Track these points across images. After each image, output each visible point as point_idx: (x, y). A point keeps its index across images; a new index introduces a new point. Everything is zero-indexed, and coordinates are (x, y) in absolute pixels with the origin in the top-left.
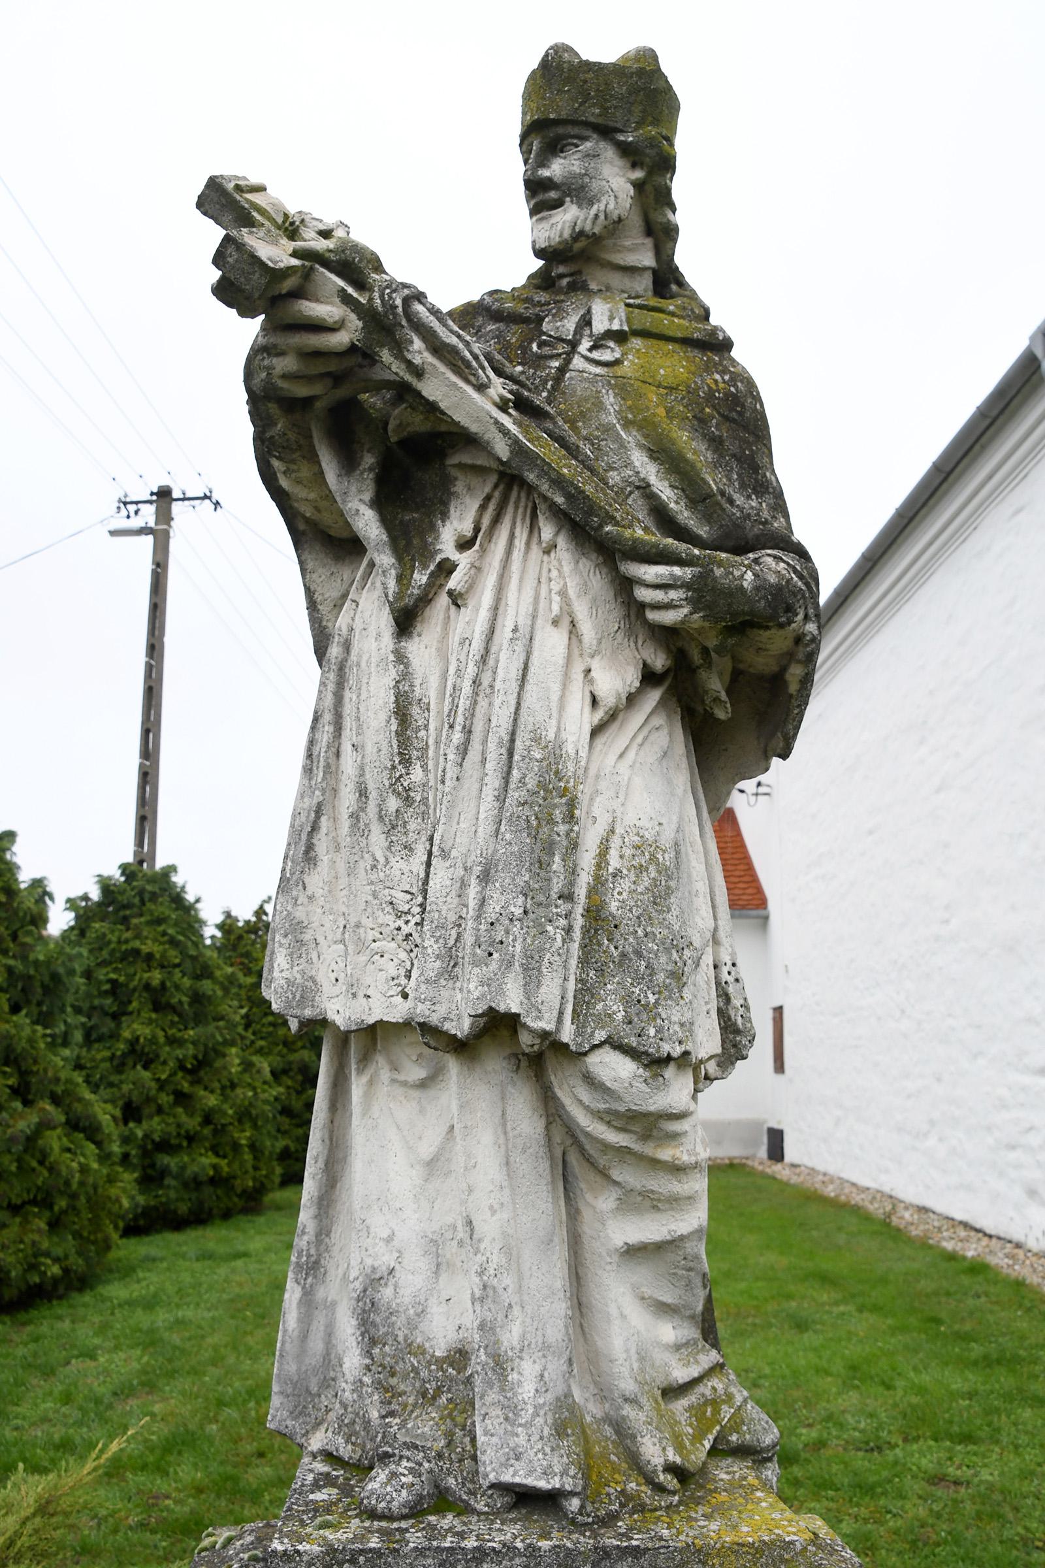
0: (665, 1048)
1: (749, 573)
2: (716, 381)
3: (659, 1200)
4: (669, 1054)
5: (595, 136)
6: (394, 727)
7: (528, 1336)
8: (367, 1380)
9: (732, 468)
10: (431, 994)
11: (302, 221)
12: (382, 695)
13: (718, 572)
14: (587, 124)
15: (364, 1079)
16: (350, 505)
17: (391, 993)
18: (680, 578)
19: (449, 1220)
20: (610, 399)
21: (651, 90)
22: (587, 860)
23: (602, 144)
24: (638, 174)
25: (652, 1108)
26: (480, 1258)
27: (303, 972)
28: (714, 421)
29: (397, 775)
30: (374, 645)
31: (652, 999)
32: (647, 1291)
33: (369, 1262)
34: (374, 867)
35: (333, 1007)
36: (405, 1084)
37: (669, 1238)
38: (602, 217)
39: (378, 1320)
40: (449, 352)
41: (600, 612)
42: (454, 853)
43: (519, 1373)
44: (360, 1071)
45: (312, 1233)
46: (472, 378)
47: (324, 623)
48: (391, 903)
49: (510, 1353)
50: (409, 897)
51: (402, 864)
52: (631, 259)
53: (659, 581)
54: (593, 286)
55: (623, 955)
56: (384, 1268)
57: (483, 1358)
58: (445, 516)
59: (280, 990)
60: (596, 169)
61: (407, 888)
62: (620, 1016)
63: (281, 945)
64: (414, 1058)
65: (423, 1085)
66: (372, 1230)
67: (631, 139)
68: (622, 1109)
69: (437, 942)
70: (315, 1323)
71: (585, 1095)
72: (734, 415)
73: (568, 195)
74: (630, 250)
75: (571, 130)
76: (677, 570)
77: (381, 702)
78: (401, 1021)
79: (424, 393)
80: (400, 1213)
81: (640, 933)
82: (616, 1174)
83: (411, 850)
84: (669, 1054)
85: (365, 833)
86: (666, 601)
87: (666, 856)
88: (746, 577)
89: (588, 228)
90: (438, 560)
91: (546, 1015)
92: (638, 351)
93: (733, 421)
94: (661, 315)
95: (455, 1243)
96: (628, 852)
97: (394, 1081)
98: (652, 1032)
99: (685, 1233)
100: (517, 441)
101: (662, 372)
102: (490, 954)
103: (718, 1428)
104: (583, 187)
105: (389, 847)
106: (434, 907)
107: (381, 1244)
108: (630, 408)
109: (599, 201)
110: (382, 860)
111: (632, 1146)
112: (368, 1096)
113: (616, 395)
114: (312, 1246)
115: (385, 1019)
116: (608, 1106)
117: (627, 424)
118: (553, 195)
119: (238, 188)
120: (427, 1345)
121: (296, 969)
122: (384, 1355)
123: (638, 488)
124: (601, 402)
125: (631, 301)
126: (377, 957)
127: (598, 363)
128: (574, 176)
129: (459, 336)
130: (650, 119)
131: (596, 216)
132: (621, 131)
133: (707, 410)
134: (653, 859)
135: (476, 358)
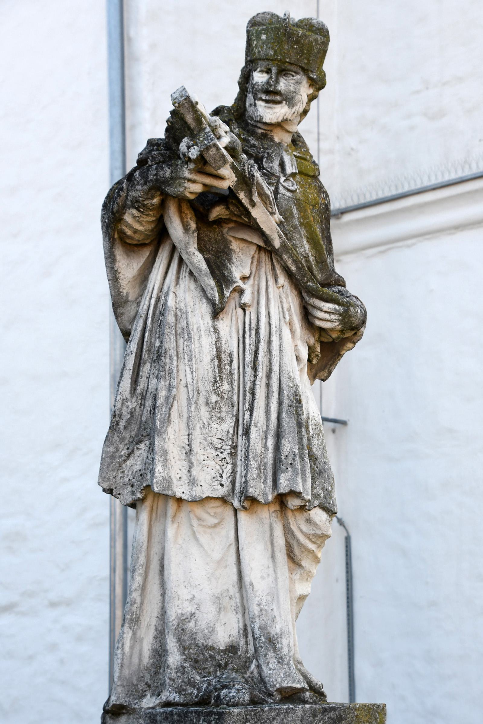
5: (302, 73)
6: (216, 363)
7: (283, 629)
8: (185, 665)
10: (255, 484)
12: (208, 346)
15: (175, 526)
16: (190, 250)
17: (213, 484)
18: (338, 311)
19: (225, 587)
26: (257, 599)
27: (167, 474)
29: (218, 385)
30: (201, 322)
33: (180, 612)
34: (204, 427)
35: (179, 490)
36: (205, 526)
39: (186, 638)
40: (266, 197)
42: (259, 425)
43: (282, 644)
44: (173, 521)
45: (139, 603)
46: (270, 209)
47: (121, 290)
48: (211, 444)
49: (276, 636)
50: (221, 441)
51: (217, 426)
53: (329, 311)
54: (277, 140)
55: (320, 471)
56: (188, 614)
57: (264, 640)
58: (230, 260)
59: (160, 482)
60: (299, 90)
61: (220, 437)
63: (159, 461)
64: (212, 514)
65: (215, 526)
66: (181, 597)
67: (315, 77)
68: (320, 533)
69: (256, 462)
70: (135, 648)
71: (304, 527)
73: (286, 100)
75: (294, 68)
76: (337, 307)
77: (208, 350)
78: (220, 496)
79: (252, 214)
80: (199, 586)
82: (303, 563)
83: (222, 420)
85: (198, 409)
86: (329, 319)
90: (235, 286)
95: (228, 597)
97: (199, 525)
100: (284, 242)
102: (287, 468)
104: (292, 98)
105: (211, 418)
106: (253, 447)
107: (186, 602)
108: (302, 217)
109: (297, 105)
110: (206, 424)
112: (177, 534)
113: (297, 209)
114: (138, 609)
115: (211, 496)
116: (314, 532)
118: (278, 98)
120: (215, 646)
121: (166, 472)
122: (190, 654)
123: (305, 257)
124: (292, 213)
126: (206, 468)
127: (289, 190)
128: (290, 92)
132: (312, 72)
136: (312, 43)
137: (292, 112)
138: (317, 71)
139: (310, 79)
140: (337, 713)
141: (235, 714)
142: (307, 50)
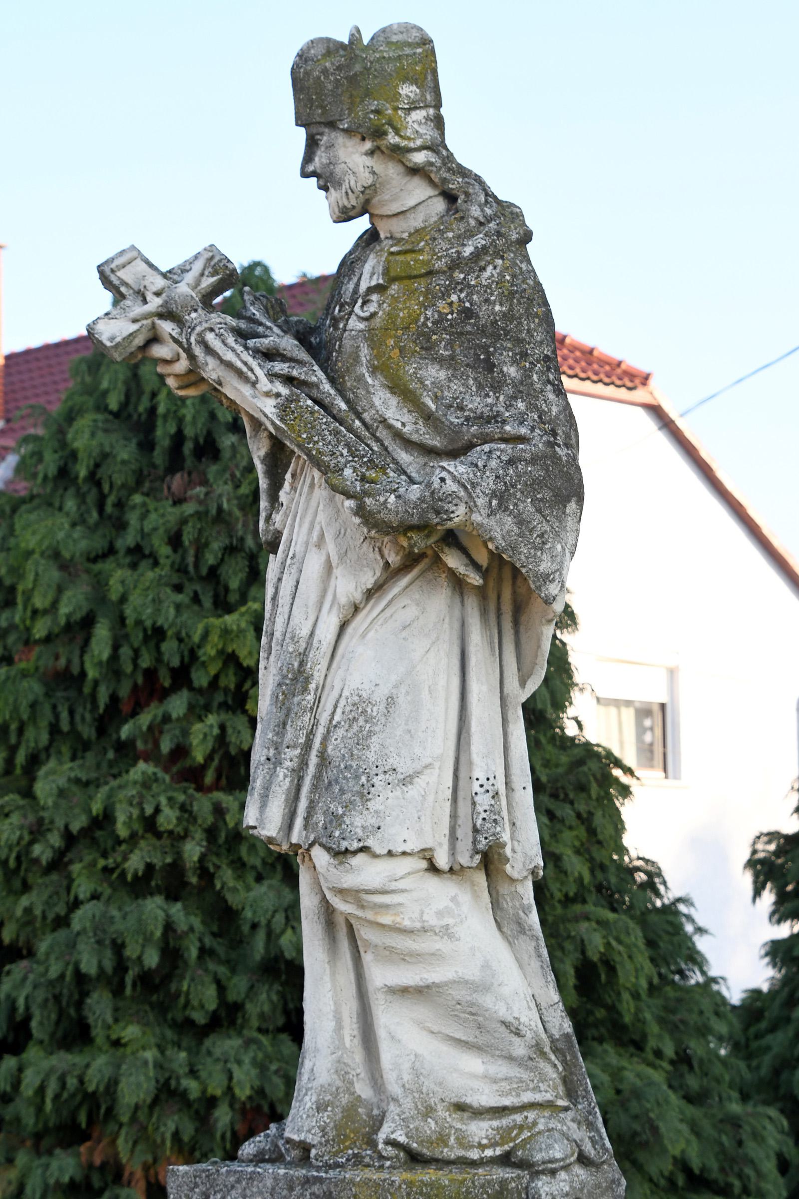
0: (344, 844)
1: (393, 496)
2: (451, 304)
3: (405, 955)
4: (347, 849)
5: (327, 130)
9: (468, 376)
11: (145, 287)
13: (368, 501)
14: (320, 123)
20: (365, 352)
21: (351, 77)
22: (324, 719)
23: (333, 135)
24: (368, 145)
25: (345, 886)
28: (443, 343)
31: (340, 811)
32: (435, 1028)
37: (421, 984)
38: (349, 191)
41: (349, 530)
52: (395, 208)
60: (335, 157)
62: (320, 824)
67: (346, 126)
72: (469, 328)
74: (391, 201)
81: (342, 766)
84: (347, 849)
87: (375, 709)
88: (389, 500)
89: (346, 203)
91: (268, 826)
92: (393, 296)
93: (469, 333)
94: (409, 257)
96: (348, 709)
98: (337, 834)
99: (437, 981)
101: (401, 314)
103: (511, 1145)
104: (331, 174)
111: (356, 913)
117: (374, 370)
119: (113, 271)
123: (381, 422)
124: (358, 356)
125: (392, 249)
129: (233, 350)
130: (358, 100)
131: (347, 193)
133: (434, 337)
134: (364, 712)
135: (245, 364)
136: (319, 78)
137: (344, 194)
138: (349, 115)
139: (346, 131)
140: (325, 1188)
141: (181, 1174)
142: (316, 94)
